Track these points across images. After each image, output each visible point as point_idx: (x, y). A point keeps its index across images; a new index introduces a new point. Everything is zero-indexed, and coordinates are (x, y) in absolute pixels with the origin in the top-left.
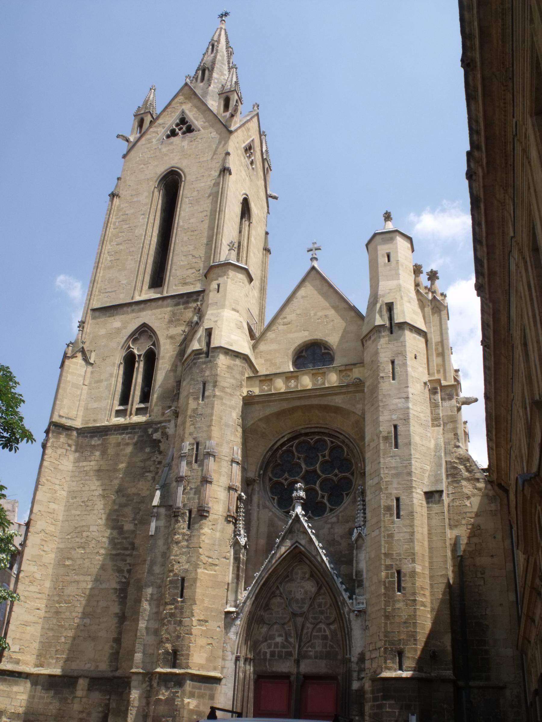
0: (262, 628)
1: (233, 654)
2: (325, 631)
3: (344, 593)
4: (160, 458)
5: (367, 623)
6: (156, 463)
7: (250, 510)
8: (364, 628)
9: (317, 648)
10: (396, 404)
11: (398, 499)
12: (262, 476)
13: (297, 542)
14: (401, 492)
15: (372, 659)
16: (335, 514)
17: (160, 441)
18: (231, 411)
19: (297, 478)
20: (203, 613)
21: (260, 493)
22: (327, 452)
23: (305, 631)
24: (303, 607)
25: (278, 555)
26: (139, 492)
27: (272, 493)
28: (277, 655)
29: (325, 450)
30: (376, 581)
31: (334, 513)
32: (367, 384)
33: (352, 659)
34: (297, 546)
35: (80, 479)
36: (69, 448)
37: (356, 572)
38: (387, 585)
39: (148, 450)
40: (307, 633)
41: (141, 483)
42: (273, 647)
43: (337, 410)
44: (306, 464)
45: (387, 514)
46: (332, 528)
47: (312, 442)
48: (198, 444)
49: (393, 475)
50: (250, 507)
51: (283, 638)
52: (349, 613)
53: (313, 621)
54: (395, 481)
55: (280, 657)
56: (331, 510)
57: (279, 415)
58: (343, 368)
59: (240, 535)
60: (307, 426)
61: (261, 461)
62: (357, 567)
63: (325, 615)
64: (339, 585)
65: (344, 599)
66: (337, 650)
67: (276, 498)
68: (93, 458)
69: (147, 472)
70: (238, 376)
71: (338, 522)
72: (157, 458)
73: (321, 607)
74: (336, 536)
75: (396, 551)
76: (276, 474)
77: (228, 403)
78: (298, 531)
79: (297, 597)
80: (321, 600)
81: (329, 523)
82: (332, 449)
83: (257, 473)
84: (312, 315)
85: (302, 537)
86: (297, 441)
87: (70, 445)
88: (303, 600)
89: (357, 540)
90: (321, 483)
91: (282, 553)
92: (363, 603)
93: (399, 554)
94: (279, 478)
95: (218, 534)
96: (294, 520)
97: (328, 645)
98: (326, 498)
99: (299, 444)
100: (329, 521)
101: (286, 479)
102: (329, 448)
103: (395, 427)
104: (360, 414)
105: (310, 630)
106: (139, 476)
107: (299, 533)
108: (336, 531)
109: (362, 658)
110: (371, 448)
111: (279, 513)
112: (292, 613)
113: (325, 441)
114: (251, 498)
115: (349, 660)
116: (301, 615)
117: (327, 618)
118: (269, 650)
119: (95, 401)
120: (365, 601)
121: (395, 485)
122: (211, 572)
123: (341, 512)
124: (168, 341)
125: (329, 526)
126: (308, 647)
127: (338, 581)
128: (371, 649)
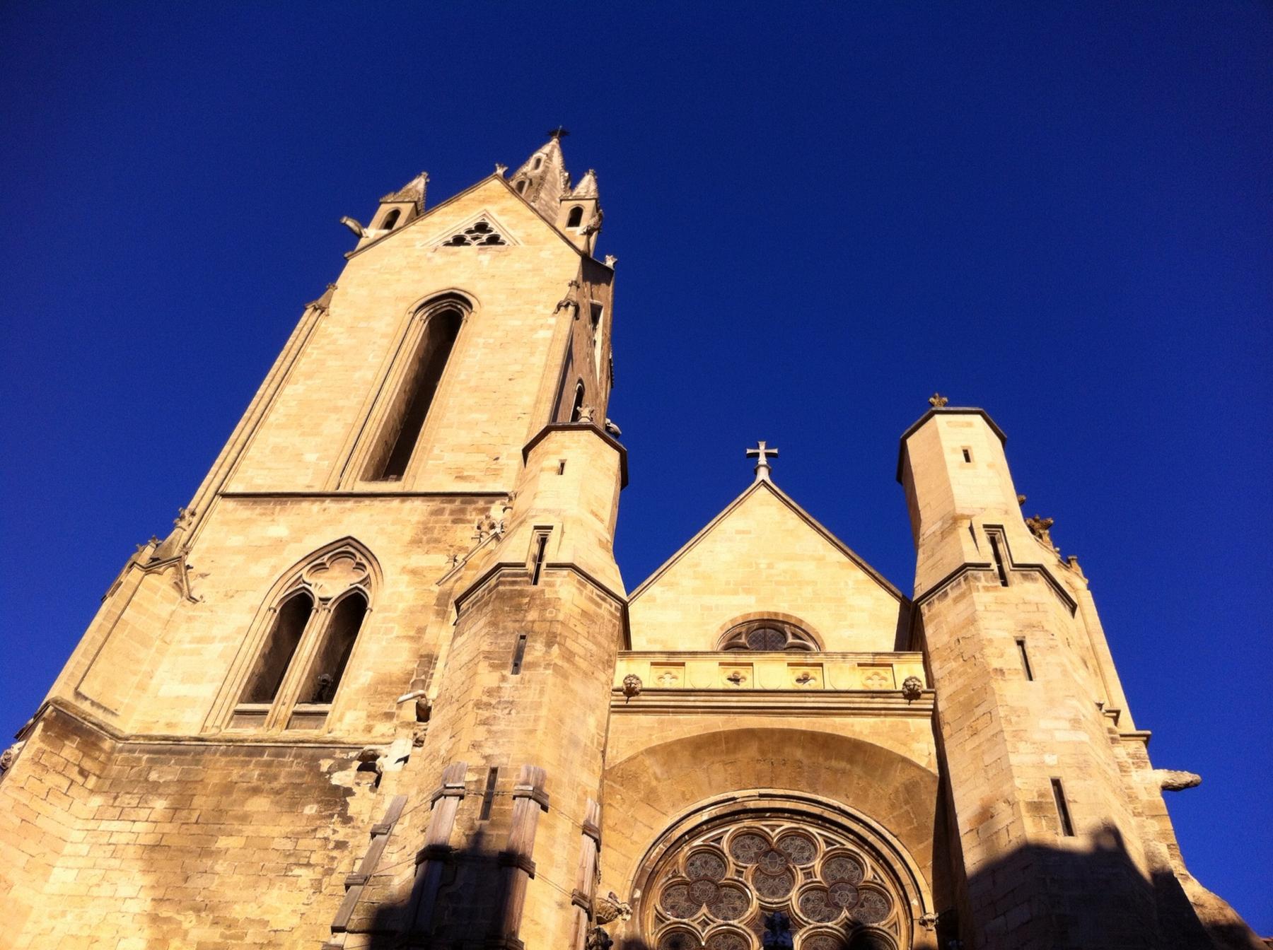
4: (342, 833)
6: (331, 845)
12: (638, 904)
17: (349, 792)
18: (585, 714)
22: (817, 864)
26: (266, 918)
35: (91, 863)
36: (80, 779)
39: (311, 809)
41: (275, 892)
43: (856, 751)
47: (773, 834)
48: (494, 771)
57: (702, 746)
58: (869, 659)
60: (763, 791)
68: (143, 813)
69: (299, 865)
72: (335, 832)
84: (762, 566)
87: (83, 773)
101: (705, 924)
103: (1056, 783)
106: (271, 875)
113: (809, 838)
119: (183, 681)
124: (406, 578)
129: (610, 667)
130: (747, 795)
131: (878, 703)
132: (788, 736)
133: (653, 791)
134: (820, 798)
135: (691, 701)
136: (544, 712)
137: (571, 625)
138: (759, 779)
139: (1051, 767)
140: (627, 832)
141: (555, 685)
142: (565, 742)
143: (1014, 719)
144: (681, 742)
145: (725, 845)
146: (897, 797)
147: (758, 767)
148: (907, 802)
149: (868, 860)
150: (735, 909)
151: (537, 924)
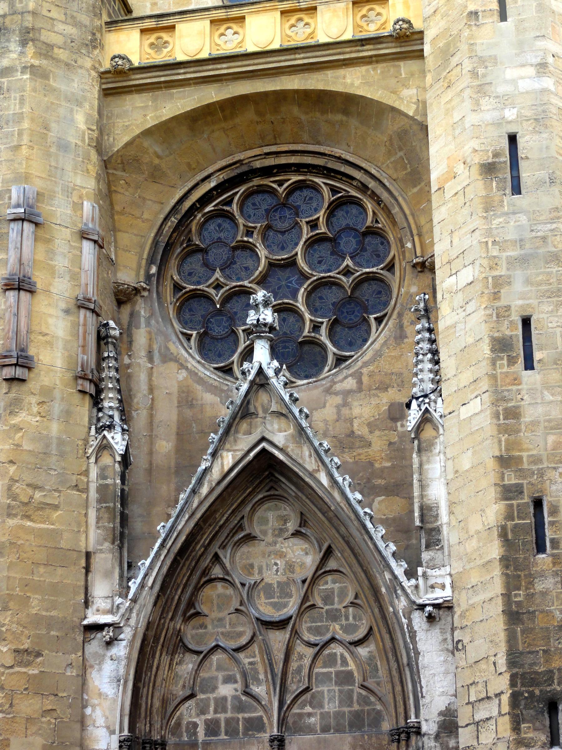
0: (180, 663)
1: (112, 732)
2: (344, 662)
3: (393, 563)
5: (458, 635)
7: (128, 366)
8: (450, 647)
9: (326, 706)
10: (514, 82)
11: (526, 322)
12: (154, 279)
13: (263, 439)
14: (534, 302)
15: (478, 723)
16: (351, 371)
18: (72, 111)
19: (246, 283)
20: (26, 632)
21: (153, 322)
22: (321, 214)
23: (294, 665)
24: (285, 605)
25: (216, 474)
27: (184, 323)
28: (223, 729)
29: (316, 210)
30: (480, 527)
31: (348, 367)
32: (428, 37)
33: (425, 728)
34: (264, 450)
37: (422, 508)
38: (510, 537)
40: (299, 670)
42: (212, 709)
43: (348, 103)
44: (267, 247)
45: (502, 359)
46: (345, 404)
47: (280, 190)
49: (511, 262)
50: (126, 360)
51: (239, 686)
52: (410, 613)
53: (313, 639)
54: (519, 275)
55: (232, 731)
56: (340, 360)
59: (110, 427)
60: (267, 150)
61: (150, 241)
62: (422, 496)
63: (344, 622)
64: (381, 545)
65: (396, 577)
66: (379, 707)
67: (194, 333)
70: (84, 19)
71: (360, 389)
73: (333, 604)
74: (355, 425)
75: (528, 450)
76: (190, 274)
77: (63, 87)
78: (265, 411)
79: (268, 580)
80: (329, 586)
81: (336, 394)
82: (334, 208)
83: (142, 272)
85: (276, 426)
86: (242, 189)
88: (284, 589)
89: (419, 428)
90: (309, 294)
91: (226, 468)
92: (443, 587)
93: (536, 460)
94: (199, 283)
95: (55, 428)
96: (252, 383)
97: (355, 698)
98: (324, 330)
99: (248, 195)
100: (338, 387)
102: (326, 205)
103: (513, 139)
104: (411, 114)
105: (307, 662)
107: (269, 418)
108: (356, 411)
109: (449, 725)
110: (449, 194)
111: (207, 372)
112: (258, 619)
113: (315, 188)
114: (130, 335)
115: (418, 732)
116: (281, 624)
117: (347, 629)
118: (203, 717)
120: (448, 581)
121: (518, 286)
122: (42, 526)
123: (366, 364)
125: (338, 400)
126: (303, 706)
127: (378, 533)
128: (473, 699)
129: (95, 47)
130: (251, 155)
131: (368, 51)
132: (282, 96)
133: (157, 168)
134: (321, 149)
135: (181, 75)
136: (26, 125)
137: (45, 12)
138: (262, 138)
139: (510, 122)
140: (137, 213)
141: (34, 90)
142: (53, 150)
143: (481, 71)
144: (175, 119)
145: (234, 208)
146: (392, 144)
147: (259, 127)
148: (401, 149)
149: (369, 206)
150: (247, 269)
151: (46, 334)
